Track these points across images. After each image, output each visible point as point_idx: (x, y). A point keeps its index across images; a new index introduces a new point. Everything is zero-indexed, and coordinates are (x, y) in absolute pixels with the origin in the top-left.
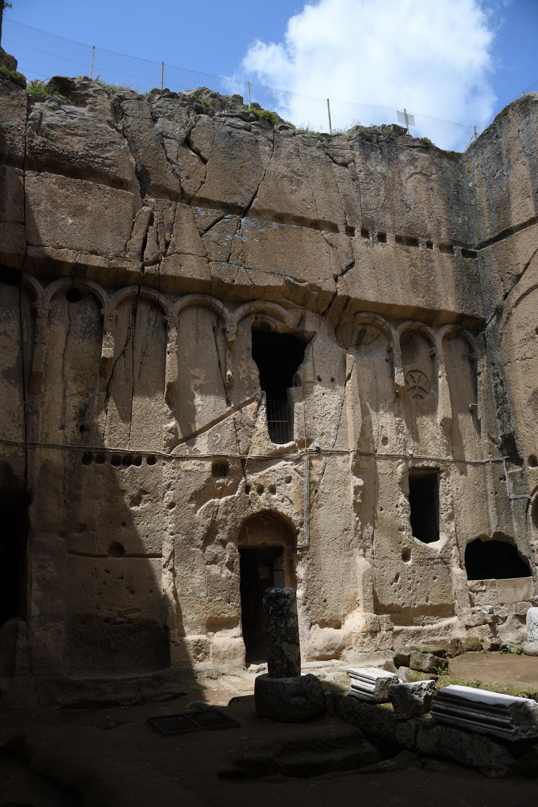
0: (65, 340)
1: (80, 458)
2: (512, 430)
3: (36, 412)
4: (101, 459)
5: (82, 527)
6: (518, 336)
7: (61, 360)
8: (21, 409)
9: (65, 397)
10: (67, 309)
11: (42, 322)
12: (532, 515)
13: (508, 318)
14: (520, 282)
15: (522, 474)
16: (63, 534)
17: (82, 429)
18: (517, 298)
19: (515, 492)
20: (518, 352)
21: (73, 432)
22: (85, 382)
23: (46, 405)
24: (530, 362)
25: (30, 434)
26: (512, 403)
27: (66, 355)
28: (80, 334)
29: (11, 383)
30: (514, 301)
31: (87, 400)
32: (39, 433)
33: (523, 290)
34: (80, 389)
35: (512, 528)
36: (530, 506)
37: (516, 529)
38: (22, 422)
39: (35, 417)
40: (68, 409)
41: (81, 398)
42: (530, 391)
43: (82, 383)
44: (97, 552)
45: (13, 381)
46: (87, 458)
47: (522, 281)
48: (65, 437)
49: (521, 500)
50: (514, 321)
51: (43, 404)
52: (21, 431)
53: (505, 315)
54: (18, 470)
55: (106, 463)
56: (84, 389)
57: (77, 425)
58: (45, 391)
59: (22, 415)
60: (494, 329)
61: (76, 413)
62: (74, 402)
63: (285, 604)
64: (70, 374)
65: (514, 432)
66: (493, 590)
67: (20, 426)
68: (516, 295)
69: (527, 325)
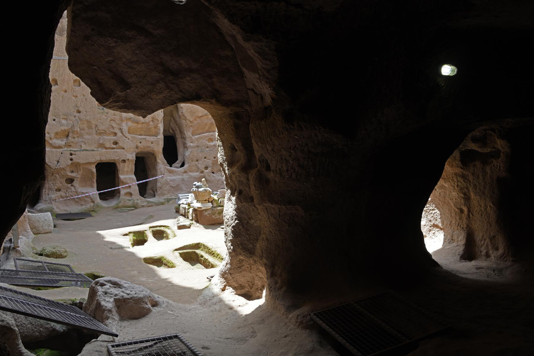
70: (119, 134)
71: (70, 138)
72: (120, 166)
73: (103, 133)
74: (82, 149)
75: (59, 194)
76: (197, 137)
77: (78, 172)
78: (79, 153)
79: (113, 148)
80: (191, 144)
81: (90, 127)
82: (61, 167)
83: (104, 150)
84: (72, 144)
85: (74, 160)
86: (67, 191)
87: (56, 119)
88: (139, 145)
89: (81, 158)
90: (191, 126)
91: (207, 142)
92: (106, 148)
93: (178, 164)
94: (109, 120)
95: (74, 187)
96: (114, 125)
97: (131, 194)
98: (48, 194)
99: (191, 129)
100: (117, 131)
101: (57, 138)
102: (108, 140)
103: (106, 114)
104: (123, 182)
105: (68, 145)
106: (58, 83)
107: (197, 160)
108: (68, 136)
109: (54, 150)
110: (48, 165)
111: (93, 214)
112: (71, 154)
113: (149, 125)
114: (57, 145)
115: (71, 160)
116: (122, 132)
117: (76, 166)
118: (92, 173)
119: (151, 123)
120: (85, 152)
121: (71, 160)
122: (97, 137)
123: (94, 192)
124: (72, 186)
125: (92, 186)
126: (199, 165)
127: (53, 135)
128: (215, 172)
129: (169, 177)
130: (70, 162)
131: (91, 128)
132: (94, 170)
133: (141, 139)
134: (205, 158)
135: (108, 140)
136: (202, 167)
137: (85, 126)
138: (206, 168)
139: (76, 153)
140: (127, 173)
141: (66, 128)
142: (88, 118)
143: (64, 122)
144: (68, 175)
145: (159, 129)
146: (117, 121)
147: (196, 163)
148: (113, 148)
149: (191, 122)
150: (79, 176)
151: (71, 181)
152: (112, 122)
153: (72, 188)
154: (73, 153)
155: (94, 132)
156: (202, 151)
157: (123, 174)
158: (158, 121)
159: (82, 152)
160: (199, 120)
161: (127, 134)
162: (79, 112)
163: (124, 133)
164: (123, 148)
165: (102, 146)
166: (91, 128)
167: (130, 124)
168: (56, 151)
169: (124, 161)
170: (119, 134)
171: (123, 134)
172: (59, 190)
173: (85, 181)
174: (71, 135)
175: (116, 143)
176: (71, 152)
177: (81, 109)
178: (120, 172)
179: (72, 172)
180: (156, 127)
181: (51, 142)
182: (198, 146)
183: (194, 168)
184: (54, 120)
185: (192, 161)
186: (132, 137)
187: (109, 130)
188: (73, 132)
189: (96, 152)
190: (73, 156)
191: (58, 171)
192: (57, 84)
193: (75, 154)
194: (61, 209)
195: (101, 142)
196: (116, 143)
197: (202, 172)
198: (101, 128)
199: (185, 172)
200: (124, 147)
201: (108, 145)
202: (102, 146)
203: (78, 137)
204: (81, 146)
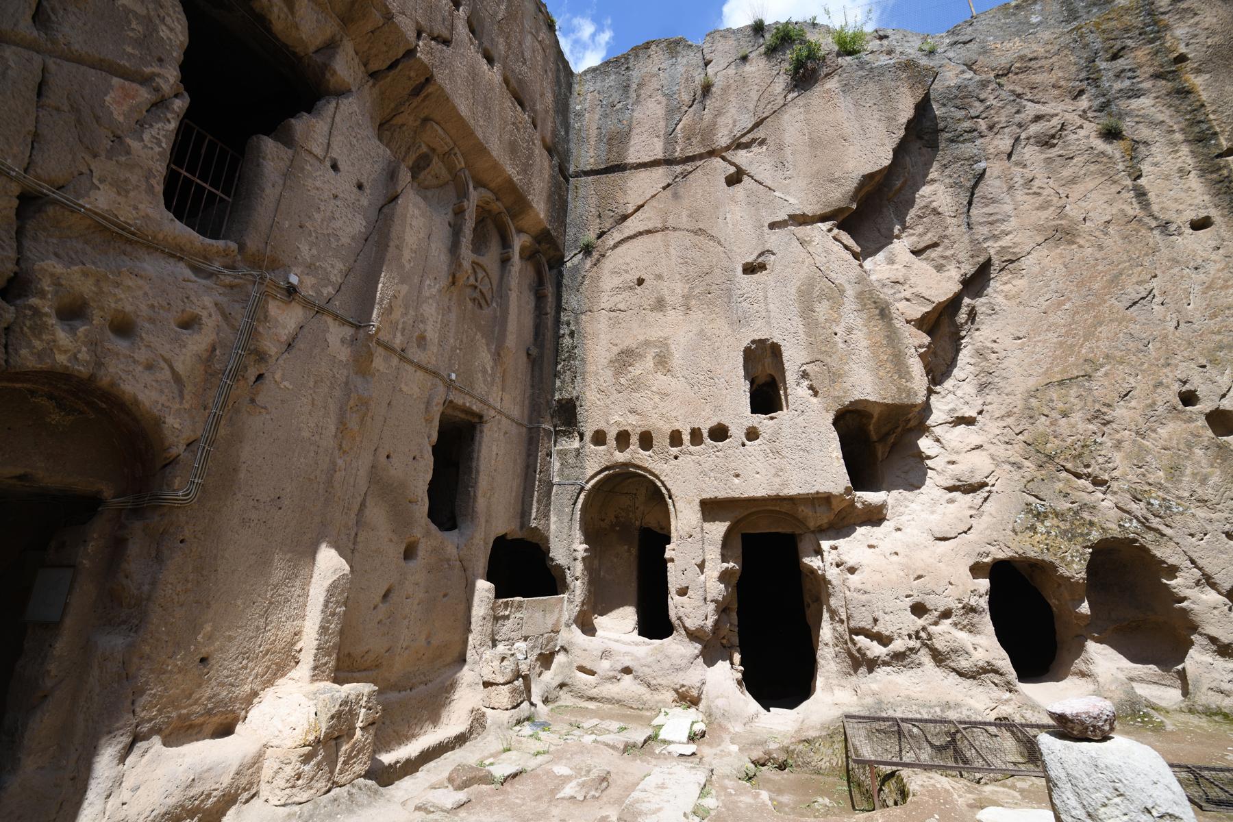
2: (575, 394)
6: (608, 282)
12: (581, 510)
13: (598, 260)
14: (625, 223)
15: (578, 453)
18: (617, 240)
19: (561, 474)
20: (606, 301)
24: (622, 315)
26: (582, 360)
30: (612, 243)
33: (627, 233)
35: (548, 525)
36: (582, 496)
37: (553, 527)
42: (616, 350)
47: (629, 222)
49: (569, 488)
50: (607, 265)
53: (596, 255)
60: (576, 269)
65: (577, 398)
66: (518, 615)
68: (617, 236)
69: (627, 272)
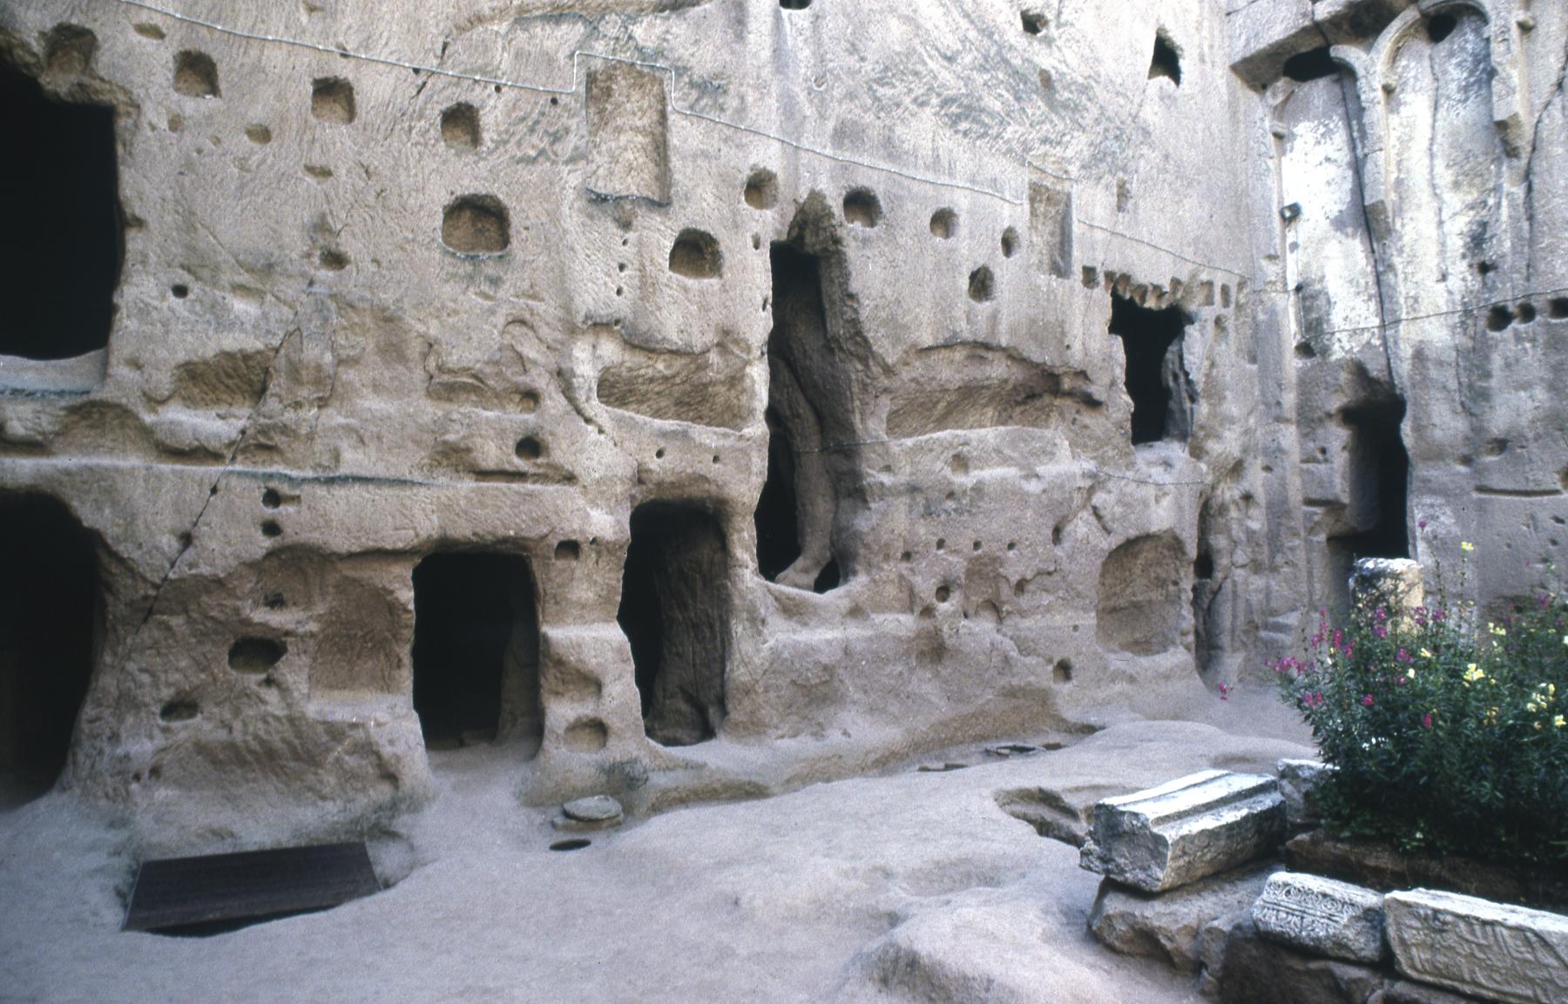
0: (1430, 121)
1: (1482, 323)
3: (1391, 267)
4: (1528, 313)
5: (1501, 445)
7: (1426, 161)
8: (1369, 269)
9: (1441, 223)
10: (1426, 63)
11: (1377, 112)
16: (1466, 460)
17: (1484, 268)
21: (1464, 279)
22: (1478, 181)
23: (1407, 249)
25: (1386, 306)
27: (1435, 148)
28: (1458, 97)
29: (1347, 235)
31: (1484, 212)
32: (1402, 300)
34: (1469, 199)
38: (1373, 290)
39: (1391, 276)
40: (1449, 242)
41: (1472, 213)
43: (1471, 185)
44: (1531, 486)
45: (1350, 230)
46: (1500, 318)
48: (1450, 293)
51: (1401, 251)
52: (1373, 305)
54: (1375, 369)
55: (1538, 318)
56: (1475, 195)
57: (1471, 266)
58: (1403, 226)
59: (1371, 280)
61: (1466, 244)
62: (1459, 225)
63: (1394, 591)
64: (1445, 176)
67: (1370, 299)
70: (554, 402)
71: (272, 404)
72: (551, 575)
73: (465, 388)
74: (343, 470)
75: (184, 730)
76: (909, 442)
77: (309, 604)
78: (321, 491)
79: (519, 476)
80: (886, 478)
81: (393, 351)
82: (205, 570)
83: (468, 484)
84: (278, 439)
85: (288, 530)
86: (237, 712)
87: (195, 289)
88: (654, 464)
89: (336, 518)
90: (886, 390)
91: (948, 471)
92: (483, 474)
93: (806, 571)
94: (500, 320)
95: (284, 690)
96: (531, 351)
97: (599, 729)
98: (115, 738)
99: (885, 405)
100: (541, 381)
101: (190, 402)
102: (491, 431)
103: (485, 288)
104: (560, 663)
105: (259, 444)
106: (223, 86)
107: (907, 556)
108: (258, 393)
109: (166, 467)
110: (121, 561)
111: (386, 858)
112: (273, 498)
113: (705, 367)
114: (187, 441)
115: (271, 528)
116: (568, 391)
117: (294, 564)
118: (393, 608)
119: (714, 357)
120: (357, 492)
121: (271, 528)
122: (431, 411)
123: (391, 717)
124: (269, 682)
125: (386, 684)
126: (917, 580)
127: (163, 381)
128: (971, 612)
129: (781, 634)
130: (267, 543)
131: (402, 358)
132: (407, 595)
133: (664, 434)
134: (941, 544)
135: (491, 431)
136: (926, 587)
137: (368, 343)
138: (944, 592)
139: (305, 491)
140: (584, 613)
141: (253, 344)
142: (387, 297)
143: (242, 307)
144: (247, 622)
145: (753, 395)
146: (544, 331)
147: (904, 567)
148: (519, 476)
149: (888, 371)
150: (313, 627)
151: (261, 651)
152: (517, 330)
153: (272, 695)
154: (285, 489)
155: (419, 374)
156: (928, 513)
157: (559, 620)
158: (749, 350)
159: (340, 492)
160: (918, 368)
161: (595, 401)
162: (335, 260)
163: (581, 396)
164: (570, 478)
165: (455, 457)
166: (402, 358)
167: (610, 350)
168: (181, 475)
169: (570, 548)
170: (554, 402)
171: (571, 400)
172: (181, 707)
173: (349, 648)
174: (277, 384)
175: (530, 446)
176: (273, 484)
177: (349, 245)
178: (546, 609)
179: (276, 602)
180: (735, 380)
181: (148, 418)
182: (913, 489)
183: (891, 591)
184: (181, 291)
185: (887, 557)
186: (619, 421)
187: (499, 374)
188: (294, 372)
189: (423, 490)
190: (285, 511)
191: (181, 595)
192: (214, 90)
193: (295, 499)
194: (188, 821)
195: (451, 437)
196: (530, 446)
197: (928, 612)
198: (463, 355)
199: (856, 612)
200: (578, 471)
201: (493, 452)
202: (455, 457)
203: (322, 403)
204: (337, 457)
